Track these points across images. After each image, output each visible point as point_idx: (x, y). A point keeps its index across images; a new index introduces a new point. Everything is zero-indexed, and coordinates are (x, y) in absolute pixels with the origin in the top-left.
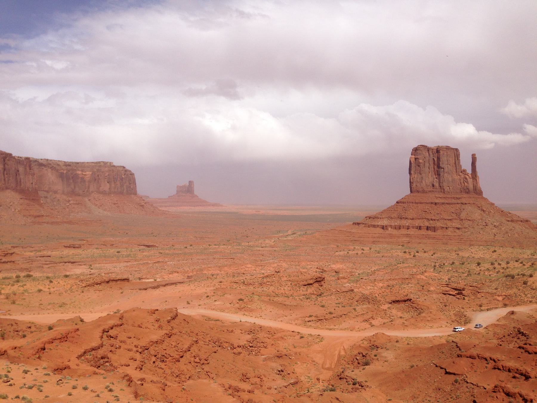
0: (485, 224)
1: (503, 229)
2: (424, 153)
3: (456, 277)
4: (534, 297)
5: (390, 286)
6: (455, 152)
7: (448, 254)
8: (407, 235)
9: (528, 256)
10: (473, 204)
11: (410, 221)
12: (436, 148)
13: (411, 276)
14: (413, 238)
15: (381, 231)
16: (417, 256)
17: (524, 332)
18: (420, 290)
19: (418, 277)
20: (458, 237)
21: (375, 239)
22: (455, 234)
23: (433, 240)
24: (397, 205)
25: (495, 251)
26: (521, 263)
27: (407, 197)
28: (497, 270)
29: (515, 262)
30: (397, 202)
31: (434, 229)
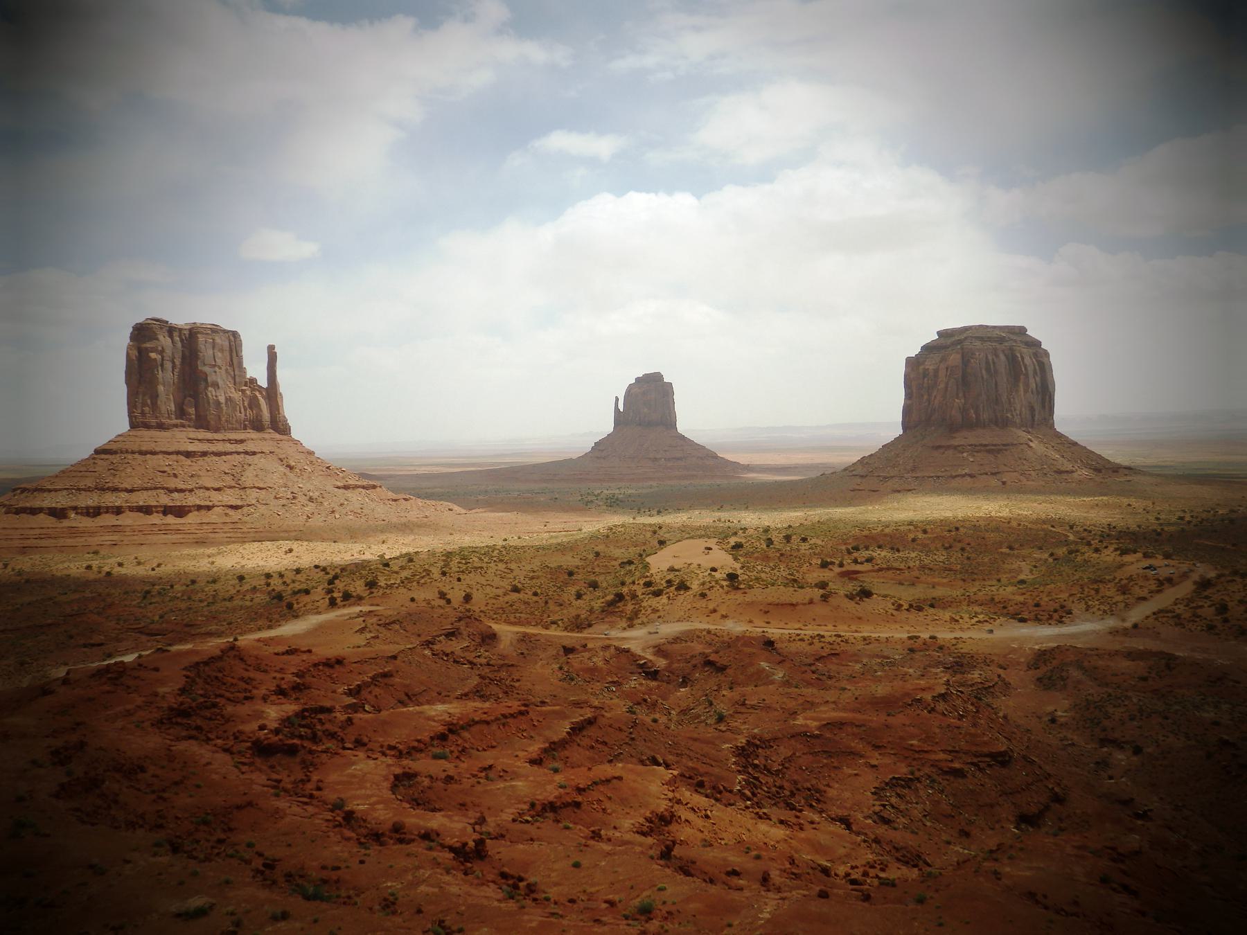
0: (290, 496)
1: (325, 504)
2: (161, 337)
6: (232, 338)
8: (116, 529)
11: (124, 495)
12: (188, 327)
15: (50, 521)
20: (232, 526)
21: (27, 543)
23: (174, 536)
24: (94, 459)
25: (291, 551)
27: (121, 439)
30: (97, 452)
31: (180, 512)
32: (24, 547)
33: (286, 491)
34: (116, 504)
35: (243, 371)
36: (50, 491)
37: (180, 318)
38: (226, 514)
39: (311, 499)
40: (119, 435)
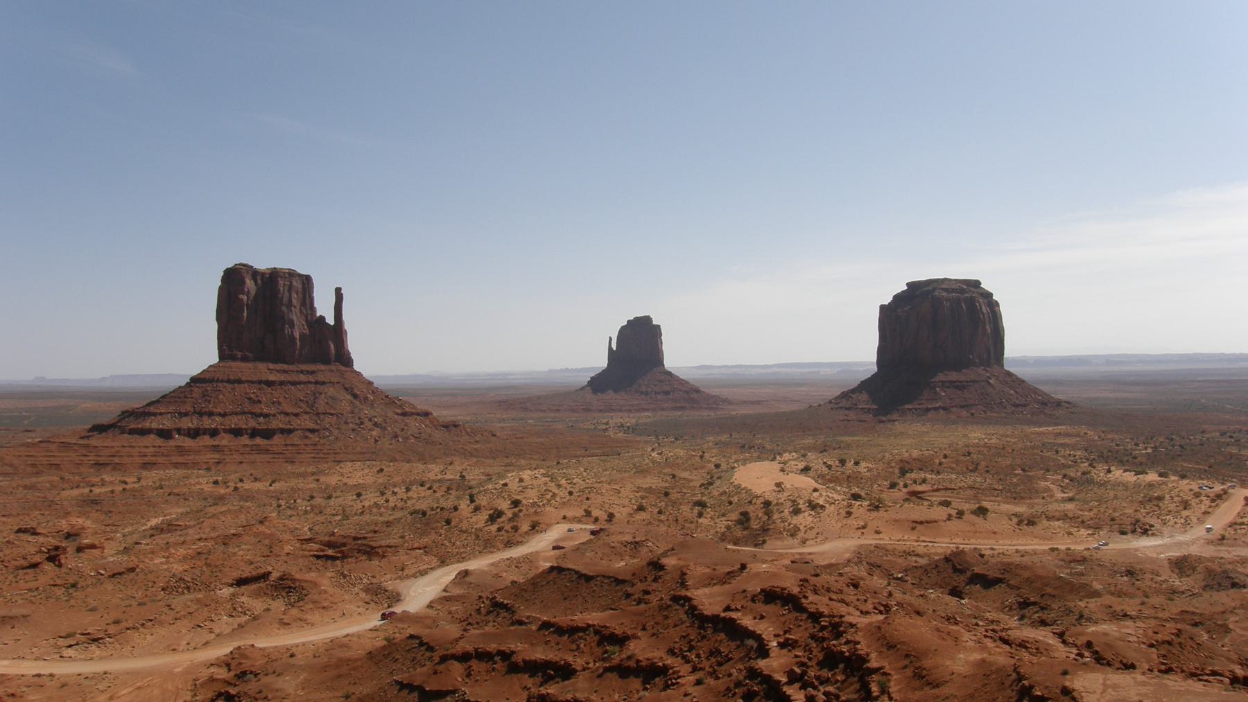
1: (389, 429)
3: (323, 523)
4: (467, 545)
5: (204, 552)
7: (300, 481)
8: (215, 448)
9: (436, 475)
10: (338, 383)
12: (269, 272)
13: (240, 529)
14: (225, 453)
15: (159, 441)
16: (241, 489)
17: (505, 602)
18: (265, 554)
19: (255, 530)
20: (312, 447)
21: (146, 459)
22: (308, 442)
23: (265, 456)
25: (382, 470)
26: (430, 488)
27: (212, 369)
28: (391, 504)
29: (420, 488)
30: (195, 380)
32: (144, 464)
33: (353, 417)
34: (213, 426)
35: (313, 309)
36: (155, 414)
37: (262, 263)
38: (306, 437)
39: (376, 424)
40: (210, 366)
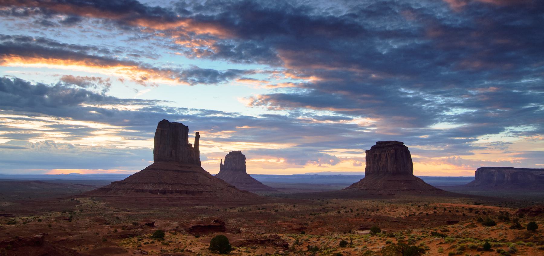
31: (193, 193)
